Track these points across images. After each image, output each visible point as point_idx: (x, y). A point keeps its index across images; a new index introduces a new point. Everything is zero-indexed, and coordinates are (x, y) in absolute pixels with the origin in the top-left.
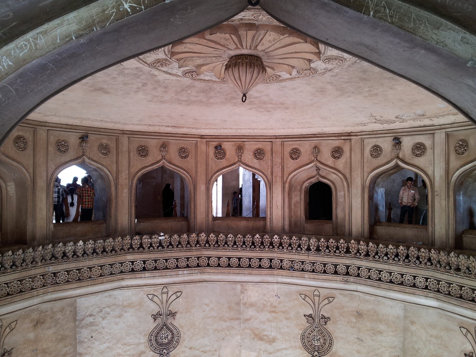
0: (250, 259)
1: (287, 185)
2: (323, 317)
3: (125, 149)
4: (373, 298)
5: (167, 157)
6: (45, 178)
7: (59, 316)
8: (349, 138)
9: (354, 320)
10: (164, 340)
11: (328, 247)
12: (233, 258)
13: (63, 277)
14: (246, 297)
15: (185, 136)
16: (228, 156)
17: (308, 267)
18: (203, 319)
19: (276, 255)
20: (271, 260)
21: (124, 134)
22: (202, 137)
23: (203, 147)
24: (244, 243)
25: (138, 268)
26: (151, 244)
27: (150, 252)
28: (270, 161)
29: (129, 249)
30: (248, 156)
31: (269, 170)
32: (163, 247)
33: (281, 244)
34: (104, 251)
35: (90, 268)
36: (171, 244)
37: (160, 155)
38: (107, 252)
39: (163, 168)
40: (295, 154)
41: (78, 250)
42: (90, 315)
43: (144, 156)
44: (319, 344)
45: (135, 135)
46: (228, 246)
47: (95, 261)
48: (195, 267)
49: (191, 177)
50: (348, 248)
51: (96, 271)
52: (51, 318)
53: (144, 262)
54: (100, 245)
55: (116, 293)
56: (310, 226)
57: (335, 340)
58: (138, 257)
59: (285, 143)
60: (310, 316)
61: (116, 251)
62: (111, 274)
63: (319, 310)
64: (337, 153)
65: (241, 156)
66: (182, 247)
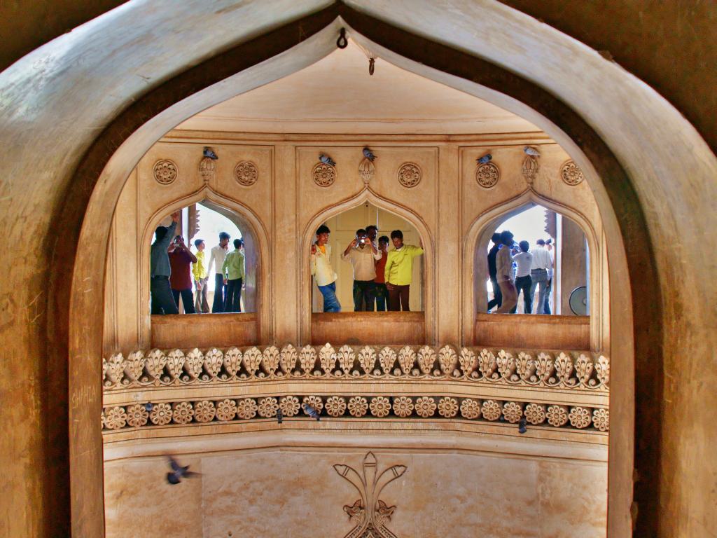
5: (374, 185)
14: (549, 491)
21: (286, 140)
22: (448, 138)
26: (337, 363)
29: (293, 371)
32: (362, 372)
34: (243, 370)
38: (248, 375)
43: (327, 184)
46: (500, 376)
48: (429, 417)
51: (227, 408)
52: (150, 488)
54: (234, 359)
61: (267, 374)
62: (258, 416)
65: (533, 177)
66: (403, 373)
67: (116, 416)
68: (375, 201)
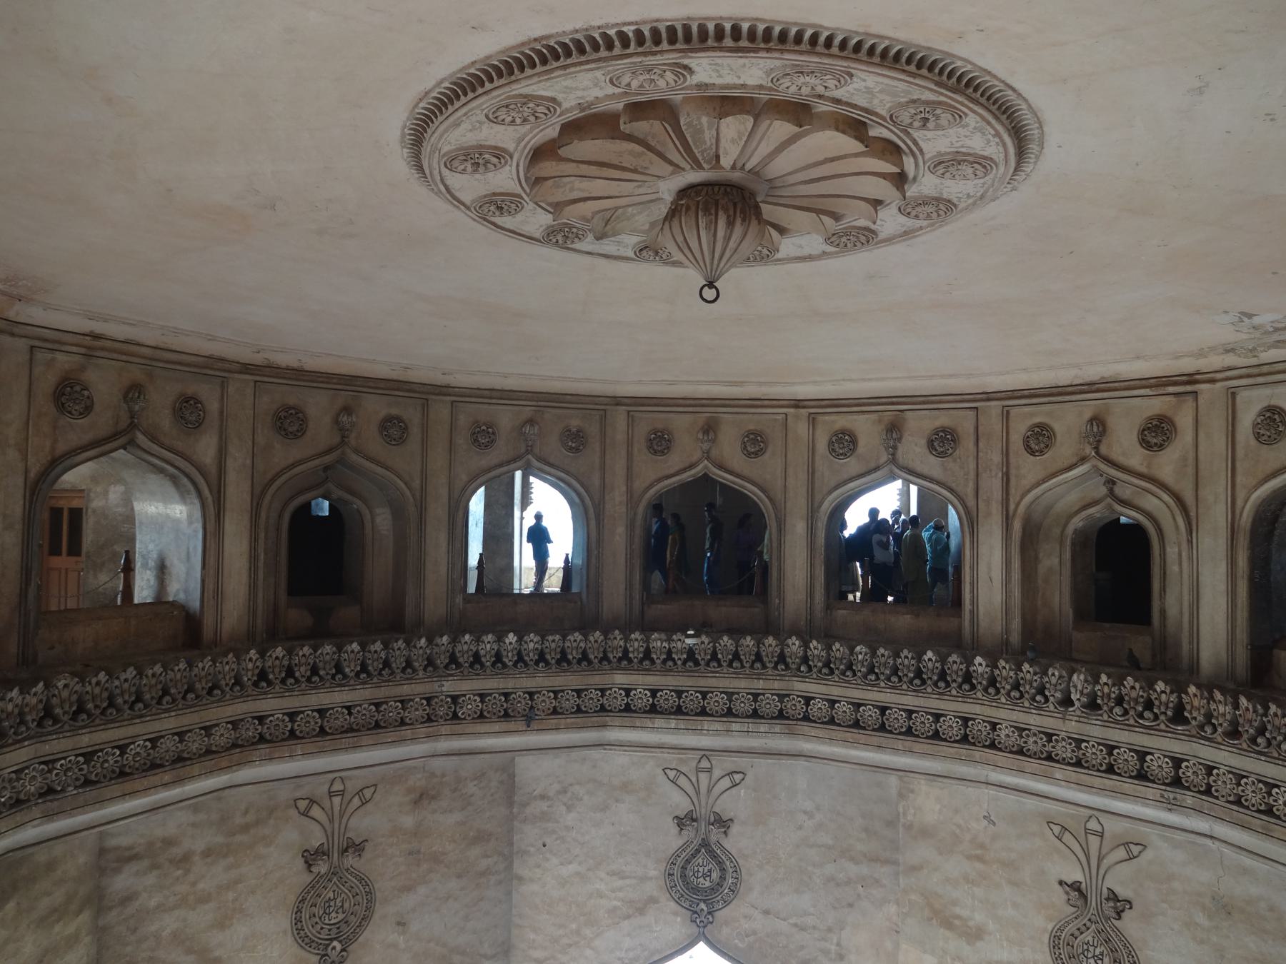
0: (910, 712)
1: (1017, 526)
2: (1113, 896)
3: (620, 436)
5: (714, 453)
6: (445, 500)
7: (471, 788)
8: (1189, 388)
9: (1201, 919)
11: (1120, 701)
12: (865, 705)
13: (470, 706)
15: (755, 403)
16: (861, 449)
19: (980, 709)
20: (966, 720)
22: (798, 404)
23: (801, 428)
24: (895, 671)
25: (639, 704)
26: (669, 652)
27: (665, 672)
29: (620, 660)
30: (914, 449)
32: (697, 663)
33: (993, 682)
38: (569, 663)
39: (706, 479)
40: (1040, 438)
41: (504, 653)
42: (543, 797)
43: (662, 453)
46: (855, 675)
47: (541, 680)
48: (773, 718)
49: (770, 499)
50: (1180, 708)
52: (455, 790)
53: (654, 693)
54: (553, 645)
55: (596, 754)
58: (641, 681)
60: (1075, 886)
61: (590, 662)
62: (579, 710)
63: (1102, 872)
64: (1157, 433)
65: (895, 448)
66: (743, 667)
67: (417, 709)
68: (717, 474)
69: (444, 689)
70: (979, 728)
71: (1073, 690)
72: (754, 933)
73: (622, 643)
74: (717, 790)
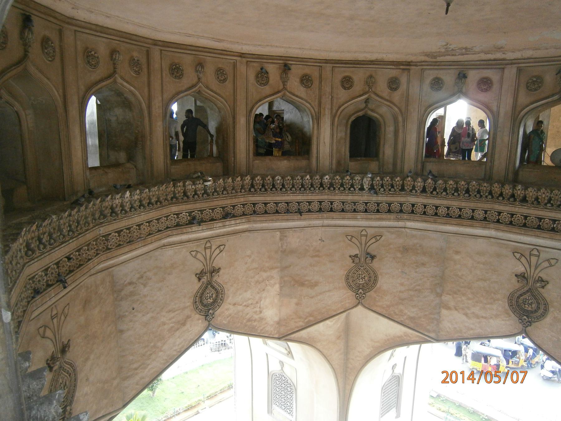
4: (420, 233)
7: (101, 290)
8: (408, 67)
9: (399, 255)
10: (209, 300)
13: (114, 239)
14: (286, 244)
15: (224, 52)
16: (271, 82)
17: (362, 208)
18: (245, 272)
19: (325, 197)
20: (320, 202)
22: (242, 55)
26: (195, 191)
27: (195, 201)
28: (317, 90)
30: (294, 83)
31: (317, 100)
32: (208, 195)
35: (139, 226)
36: (216, 191)
37: (196, 76)
40: (347, 82)
42: (131, 283)
44: (364, 282)
45: (169, 47)
46: (276, 190)
48: (241, 216)
55: (157, 253)
56: (353, 165)
57: (380, 277)
59: (336, 69)
60: (356, 256)
69: (101, 232)
70: (326, 205)
71: (364, 184)
72: (230, 315)
73: (173, 189)
74: (214, 256)
